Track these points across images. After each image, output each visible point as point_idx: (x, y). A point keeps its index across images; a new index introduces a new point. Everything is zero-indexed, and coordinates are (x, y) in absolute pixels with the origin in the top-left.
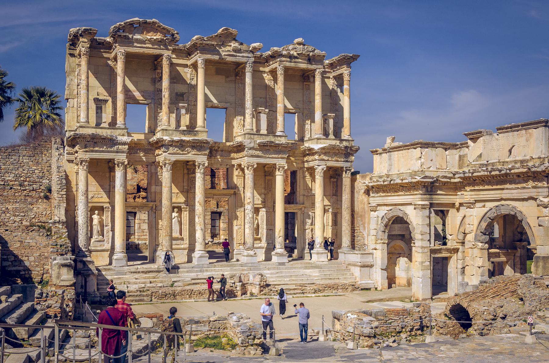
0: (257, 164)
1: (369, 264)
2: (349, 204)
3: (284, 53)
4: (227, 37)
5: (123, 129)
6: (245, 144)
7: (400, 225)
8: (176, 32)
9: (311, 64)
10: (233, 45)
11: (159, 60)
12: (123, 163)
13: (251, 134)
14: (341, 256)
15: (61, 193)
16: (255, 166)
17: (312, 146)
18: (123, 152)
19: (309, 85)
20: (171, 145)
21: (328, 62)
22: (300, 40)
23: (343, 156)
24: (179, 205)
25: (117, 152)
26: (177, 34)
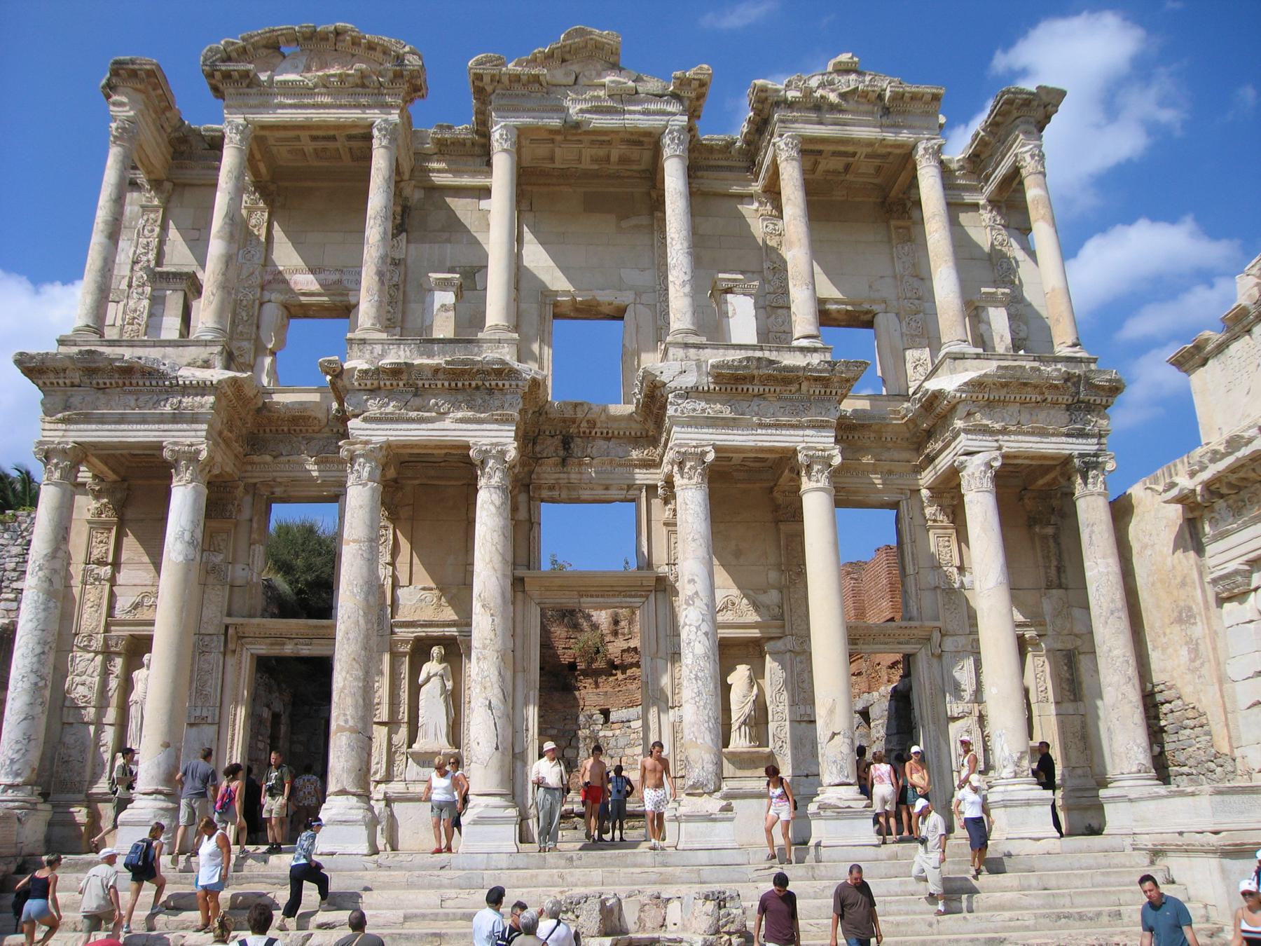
2: (1118, 595)
3: (792, 94)
4: (587, 55)
5: (206, 344)
6: (664, 378)
8: (407, 49)
9: (896, 127)
12: (193, 457)
13: (687, 346)
14: (1116, 817)
16: (710, 457)
18: (194, 419)
19: (908, 228)
20: (374, 392)
22: (845, 57)
23: (1063, 416)
25: (176, 418)
26: (412, 52)
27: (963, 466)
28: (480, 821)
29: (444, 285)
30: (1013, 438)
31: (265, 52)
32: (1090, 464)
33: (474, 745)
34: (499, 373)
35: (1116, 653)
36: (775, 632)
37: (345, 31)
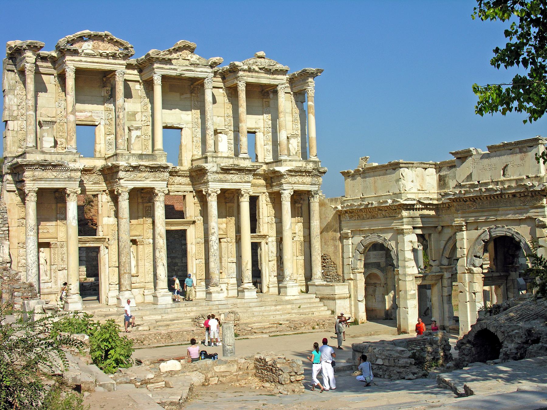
0: (221, 190)
1: (345, 295)
3: (246, 67)
7: (375, 252)
8: (130, 46)
10: (192, 60)
11: (108, 76)
13: (213, 157)
15: (2, 229)
16: (219, 192)
17: (277, 169)
19: (268, 102)
20: (128, 171)
21: (288, 76)
22: (261, 53)
24: (134, 238)
26: (132, 47)
27: (282, 193)
28: (164, 296)
29: (138, 128)
30: (296, 185)
31: (79, 39)
32: (316, 193)
33: (159, 276)
34: (164, 168)
35: (317, 247)
36: (224, 236)
37: (108, 36)
